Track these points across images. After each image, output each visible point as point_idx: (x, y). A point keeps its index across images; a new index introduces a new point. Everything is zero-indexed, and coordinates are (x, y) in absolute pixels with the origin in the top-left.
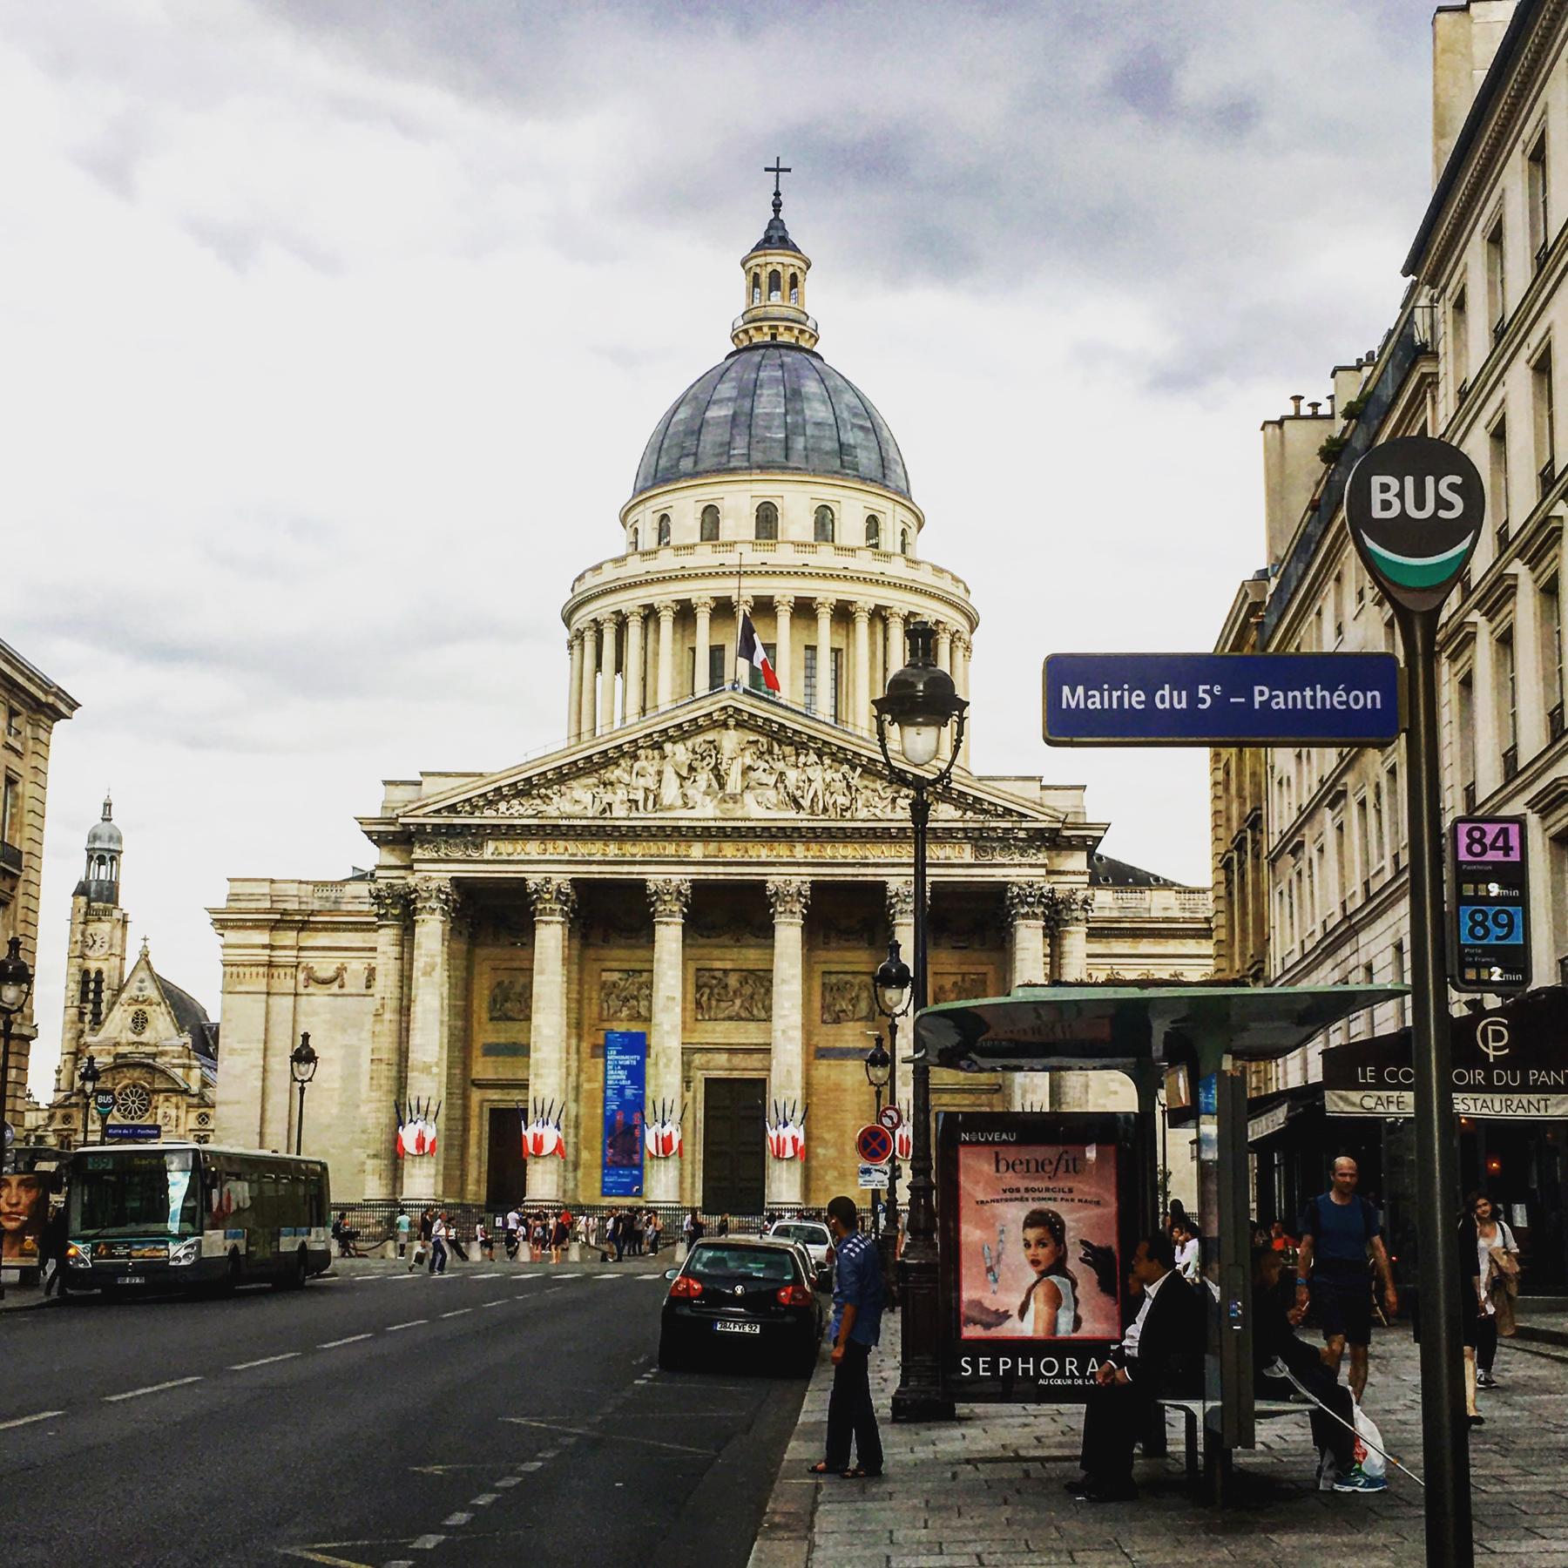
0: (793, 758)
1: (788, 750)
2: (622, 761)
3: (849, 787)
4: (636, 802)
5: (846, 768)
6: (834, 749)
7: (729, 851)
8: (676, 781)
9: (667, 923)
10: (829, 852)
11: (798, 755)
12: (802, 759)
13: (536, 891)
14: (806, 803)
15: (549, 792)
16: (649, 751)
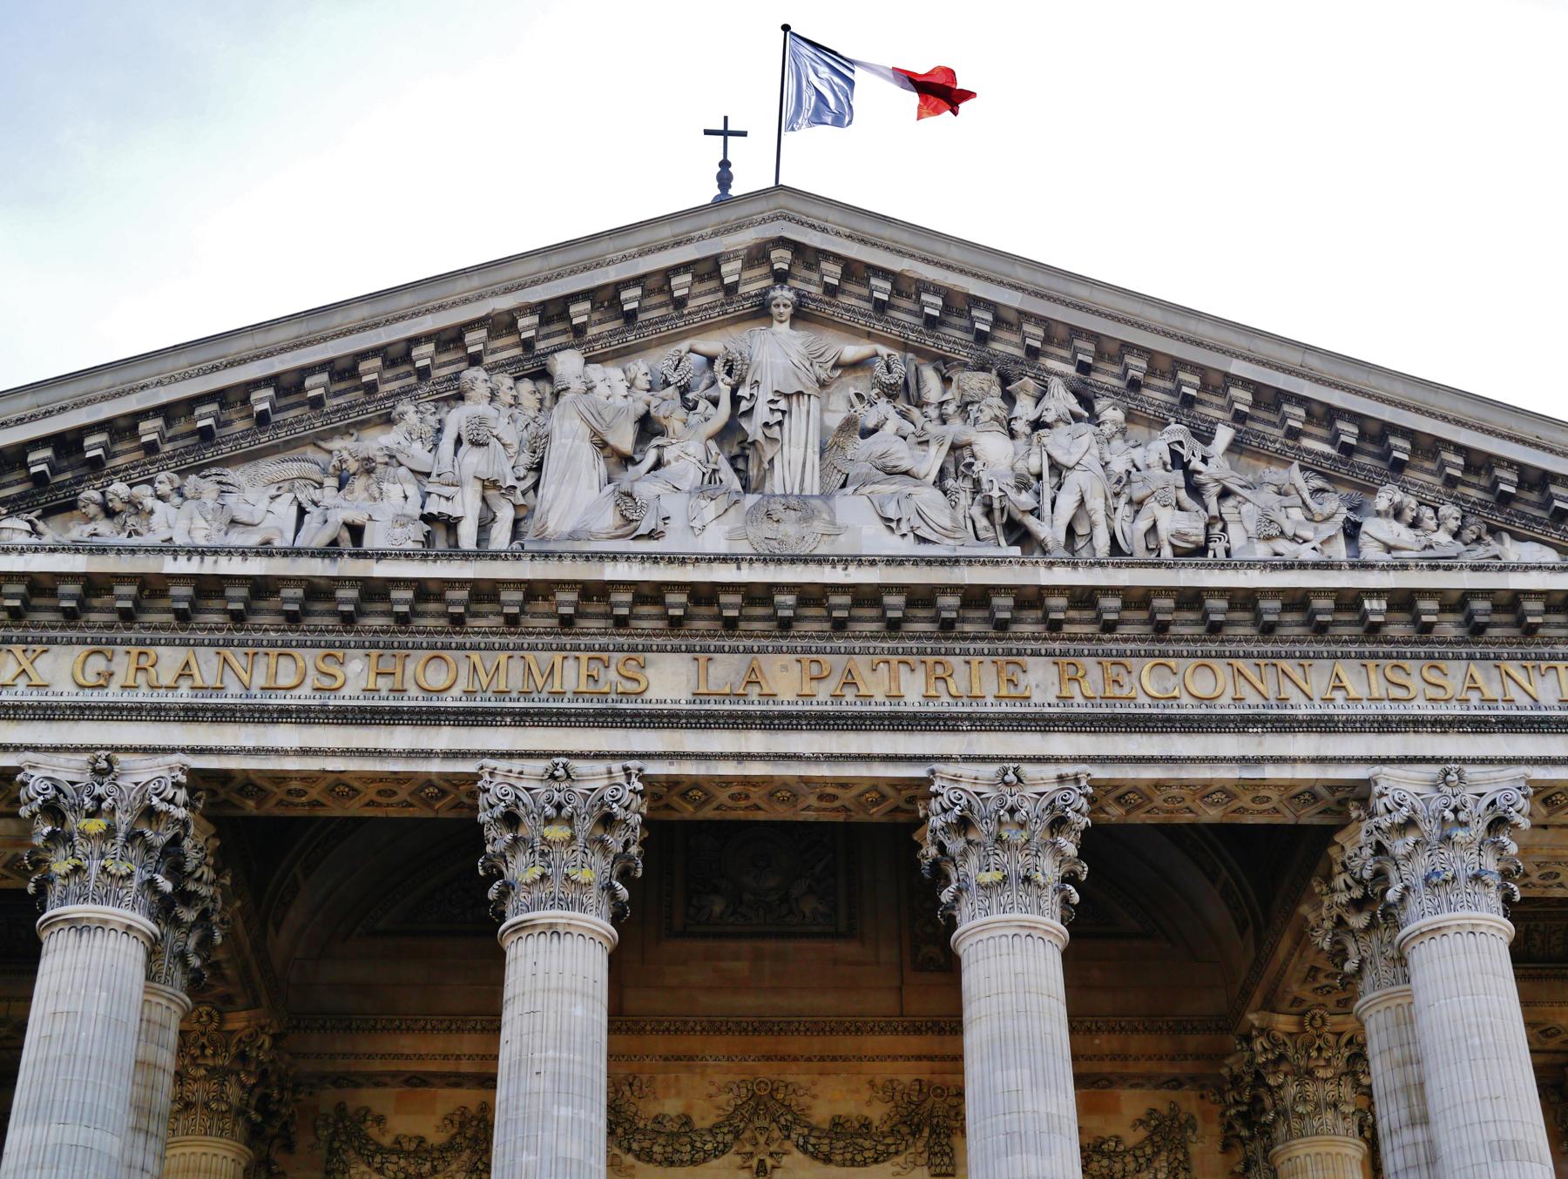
0: (993, 404)
1: (974, 381)
2: (406, 407)
3: (1195, 490)
4: (451, 525)
5: (1177, 430)
6: (1137, 366)
7: (785, 679)
8: (590, 467)
9: (553, 931)
10: (1149, 683)
11: (1009, 398)
12: (1025, 409)
13: (52, 810)
14: (1050, 531)
15: (143, 492)
16: (509, 382)
